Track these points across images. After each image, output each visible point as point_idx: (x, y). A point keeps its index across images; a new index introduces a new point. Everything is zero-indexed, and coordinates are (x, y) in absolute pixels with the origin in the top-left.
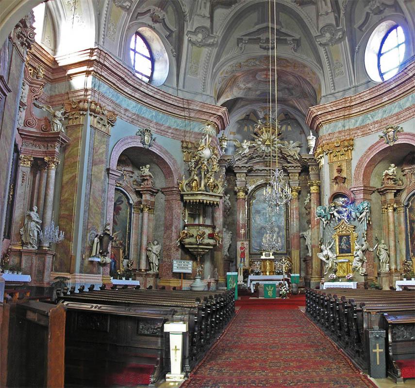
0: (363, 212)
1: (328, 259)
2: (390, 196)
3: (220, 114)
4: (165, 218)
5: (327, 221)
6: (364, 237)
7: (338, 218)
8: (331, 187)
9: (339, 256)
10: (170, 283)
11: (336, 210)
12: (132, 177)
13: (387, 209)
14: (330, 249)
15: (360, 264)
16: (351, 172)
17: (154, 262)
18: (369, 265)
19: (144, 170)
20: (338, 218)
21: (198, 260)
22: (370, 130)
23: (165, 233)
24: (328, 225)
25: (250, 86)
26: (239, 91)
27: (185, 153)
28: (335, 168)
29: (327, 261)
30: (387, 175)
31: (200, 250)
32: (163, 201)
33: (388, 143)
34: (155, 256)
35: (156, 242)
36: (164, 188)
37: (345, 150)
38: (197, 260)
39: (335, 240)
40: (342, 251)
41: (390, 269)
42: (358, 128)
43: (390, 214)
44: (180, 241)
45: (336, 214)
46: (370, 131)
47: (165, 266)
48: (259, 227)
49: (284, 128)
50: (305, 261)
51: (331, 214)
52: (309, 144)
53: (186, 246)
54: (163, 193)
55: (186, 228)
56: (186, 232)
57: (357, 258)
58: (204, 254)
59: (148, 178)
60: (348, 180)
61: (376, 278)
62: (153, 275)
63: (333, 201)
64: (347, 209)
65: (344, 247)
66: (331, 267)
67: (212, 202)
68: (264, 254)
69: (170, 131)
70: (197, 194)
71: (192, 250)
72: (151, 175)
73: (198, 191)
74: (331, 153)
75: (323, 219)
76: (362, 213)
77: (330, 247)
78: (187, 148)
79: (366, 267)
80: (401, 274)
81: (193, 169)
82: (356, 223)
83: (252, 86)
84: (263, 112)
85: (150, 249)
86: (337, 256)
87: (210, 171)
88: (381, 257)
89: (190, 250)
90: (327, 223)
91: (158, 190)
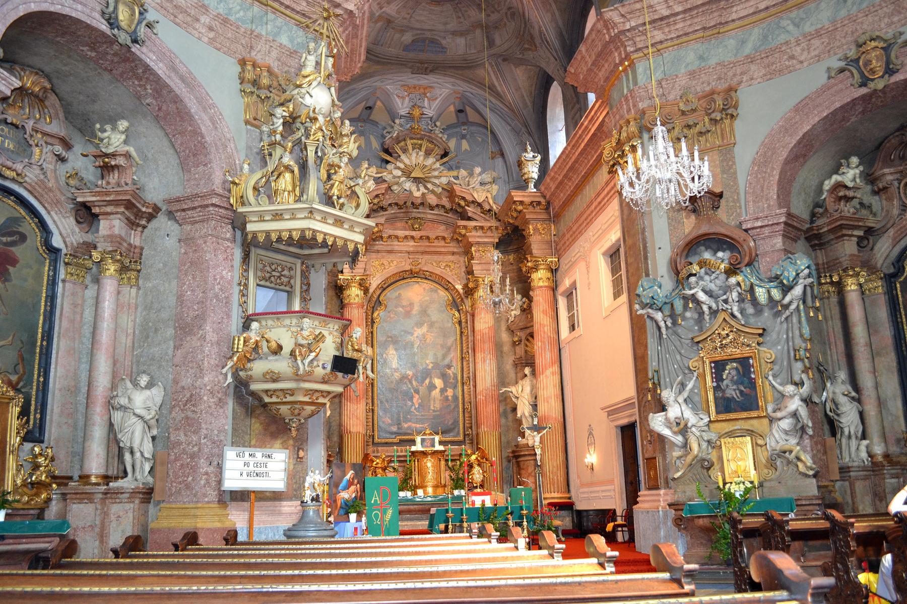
0: (796, 284)
2: (848, 248)
4: (180, 298)
7: (710, 308)
10: (196, 516)
12: (62, 159)
16: (736, 178)
17: (136, 446)
19: (109, 138)
22: (792, 57)
23: (176, 348)
25: (393, 13)
30: (840, 185)
32: (171, 243)
33: (863, 84)
34: (139, 427)
36: (178, 200)
40: (725, 406)
42: (750, 59)
45: (702, 296)
46: (794, 61)
47: (176, 460)
48: (397, 376)
51: (686, 299)
52: (526, 170)
53: (254, 387)
54: (171, 215)
55: (255, 325)
59: (121, 161)
62: (134, 493)
65: (731, 392)
67: (340, 243)
68: (418, 439)
69: (204, 19)
72: (134, 154)
77: (685, 394)
78: (255, 83)
79: (812, 450)
83: (398, 12)
84: (407, 99)
85: (123, 401)
86: (710, 421)
89: (267, 400)
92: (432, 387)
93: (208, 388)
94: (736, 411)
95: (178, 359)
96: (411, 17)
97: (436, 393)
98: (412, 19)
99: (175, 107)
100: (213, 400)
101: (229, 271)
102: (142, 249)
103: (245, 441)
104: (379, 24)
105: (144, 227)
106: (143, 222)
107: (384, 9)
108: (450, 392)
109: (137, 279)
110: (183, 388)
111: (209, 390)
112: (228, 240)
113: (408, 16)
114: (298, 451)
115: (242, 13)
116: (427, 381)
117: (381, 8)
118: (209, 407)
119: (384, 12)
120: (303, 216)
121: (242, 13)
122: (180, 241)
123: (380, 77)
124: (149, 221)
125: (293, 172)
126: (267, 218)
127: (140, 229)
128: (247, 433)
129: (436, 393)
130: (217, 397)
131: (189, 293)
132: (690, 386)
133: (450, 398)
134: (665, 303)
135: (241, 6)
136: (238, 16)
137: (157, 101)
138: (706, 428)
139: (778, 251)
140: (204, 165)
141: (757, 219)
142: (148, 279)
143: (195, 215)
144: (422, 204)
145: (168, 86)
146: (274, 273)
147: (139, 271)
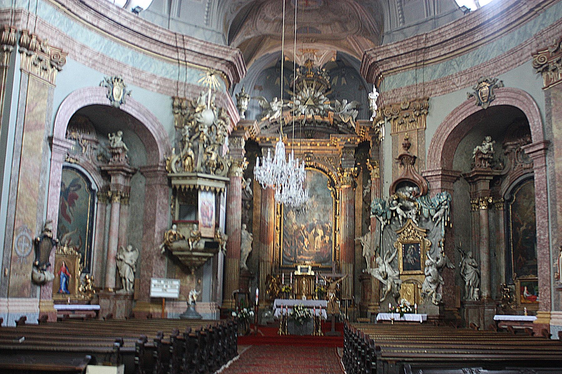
0: (440, 209)
1: (386, 278)
2: (483, 186)
3: (230, 59)
4: (145, 212)
5: (386, 221)
6: (440, 246)
7: (403, 217)
8: (394, 169)
9: (402, 275)
11: (400, 204)
12: (95, 149)
13: (478, 204)
14: (390, 263)
15: (434, 287)
17: (126, 277)
18: (448, 289)
19: (114, 139)
20: (403, 217)
21: (193, 273)
22: (454, 84)
23: (144, 234)
24: (387, 227)
26: (265, 25)
27: (177, 116)
28: (401, 141)
29: (384, 282)
30: (479, 152)
31: (194, 259)
32: (142, 185)
33: (480, 105)
34: (128, 268)
35: (130, 248)
36: (144, 167)
37: (415, 115)
38: (191, 273)
39: (398, 251)
40: (407, 267)
41: (480, 297)
42: (436, 82)
43: (483, 213)
44: (166, 246)
45: (399, 211)
46: (455, 86)
47: (143, 282)
48: (295, 227)
49: (335, 81)
50: (361, 280)
51: (392, 211)
53: (175, 253)
54: (142, 174)
56: (174, 232)
57: (429, 278)
58: (202, 265)
59: (120, 151)
60: (419, 160)
61: (459, 309)
62: (126, 296)
63: (396, 191)
64: (416, 203)
65: (410, 261)
66: (391, 290)
68: (299, 267)
69: (155, 81)
70: (191, 177)
71: (183, 259)
73: (192, 172)
74: (395, 119)
75: (381, 219)
76: (439, 210)
77: (390, 260)
78: (180, 107)
80: (498, 305)
81: (187, 139)
82: (429, 225)
84: (303, 57)
85: (121, 257)
86: (400, 275)
87: (212, 142)
88: (467, 278)
90: (387, 224)
91: (136, 170)
92: (316, 234)
94: (412, 270)
95: (144, 239)
97: (318, 238)
102: (130, 188)
104: (276, 23)
105: (131, 178)
108: (327, 238)
109: (128, 201)
110: (146, 252)
116: (313, 231)
122: (145, 185)
129: (318, 238)
132: (393, 255)
133: (327, 242)
134: (383, 213)
136: (172, 74)
138: (397, 278)
139: (439, 189)
141: (429, 171)
142: (133, 201)
144: (312, 122)
147: (129, 198)
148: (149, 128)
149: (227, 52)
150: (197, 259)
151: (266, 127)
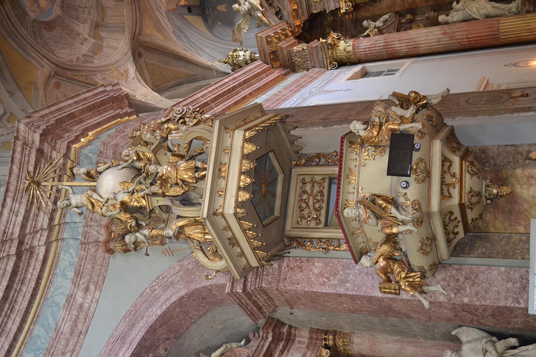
25: (88, 26)
83: (85, 21)
93: (453, 296)
96: (86, 7)
98: (88, 5)
99: (160, 329)
100: (468, 289)
101: (313, 264)
103: (521, 241)
104: (103, 34)
105: (290, 327)
106: (285, 330)
107: (87, 37)
111: (455, 294)
112: (280, 267)
113: (86, 10)
114: (531, 159)
115: (72, 251)
117: (86, 39)
118: (477, 294)
119: (89, 36)
120: (223, 220)
121: (72, 251)
123: (157, 12)
124: (283, 324)
125: (182, 227)
126: (239, 250)
127: (293, 331)
128: (510, 238)
130: (463, 283)
131: (345, 306)
135: (66, 252)
136: (74, 255)
137: (159, 345)
140: (211, 291)
143: (262, 300)
145: (139, 344)
146: (311, 204)
148: (159, 313)
149: (25, 144)
150: (455, 192)
151: (277, 14)
